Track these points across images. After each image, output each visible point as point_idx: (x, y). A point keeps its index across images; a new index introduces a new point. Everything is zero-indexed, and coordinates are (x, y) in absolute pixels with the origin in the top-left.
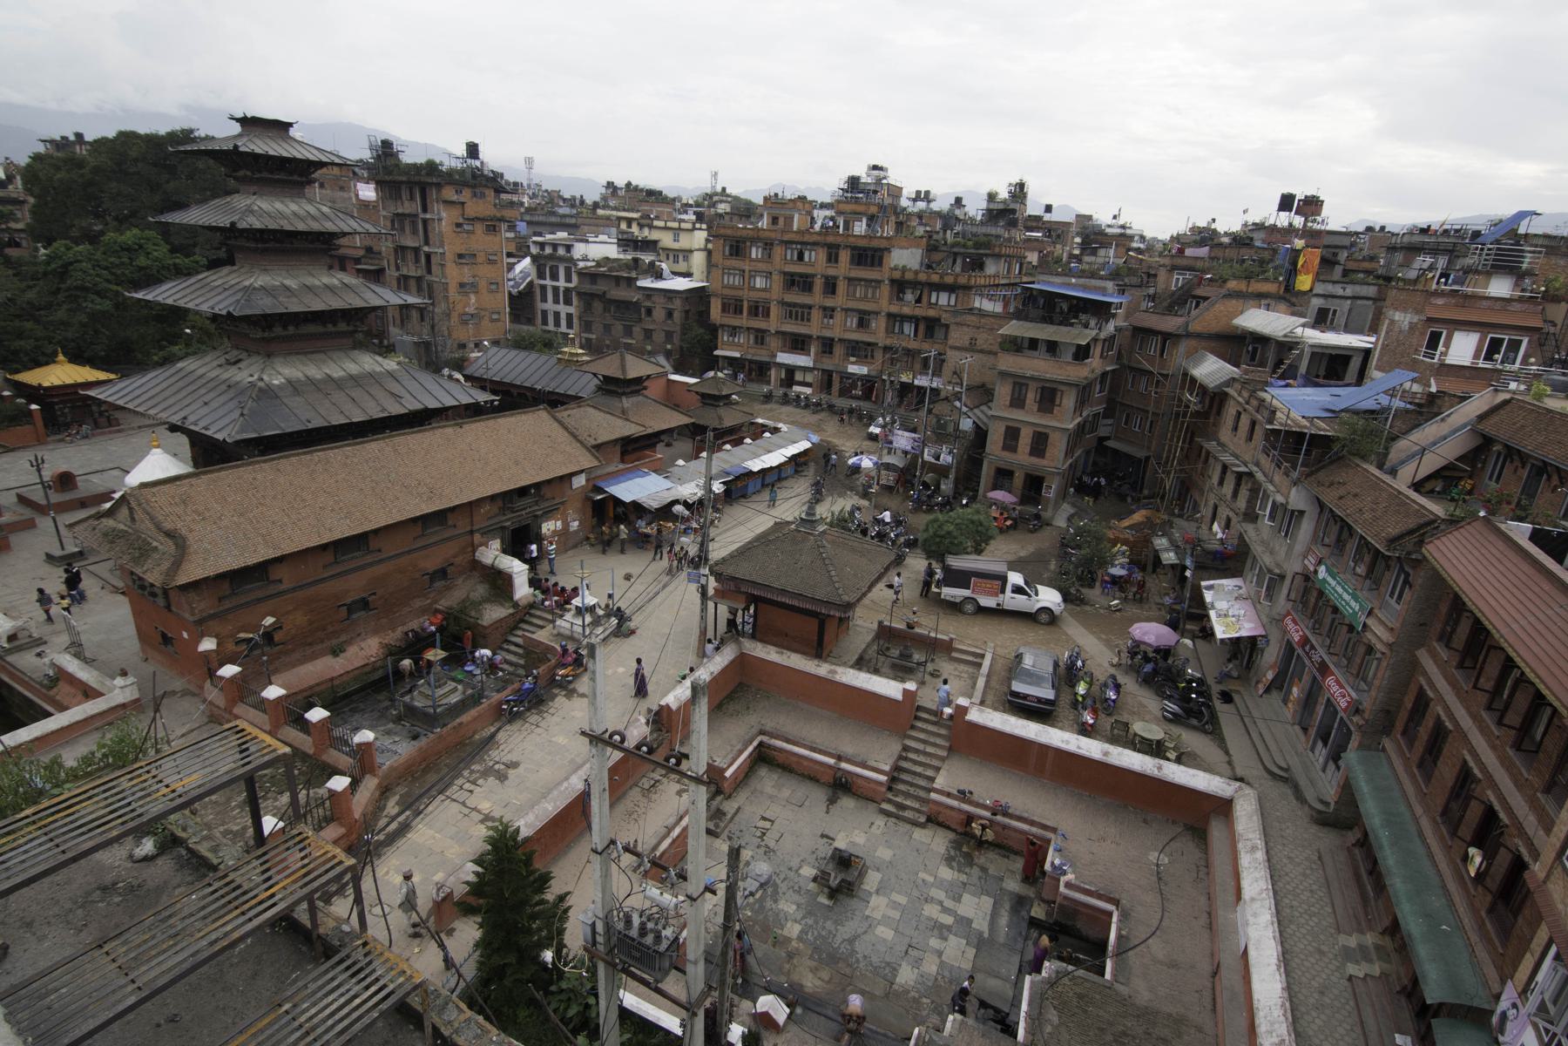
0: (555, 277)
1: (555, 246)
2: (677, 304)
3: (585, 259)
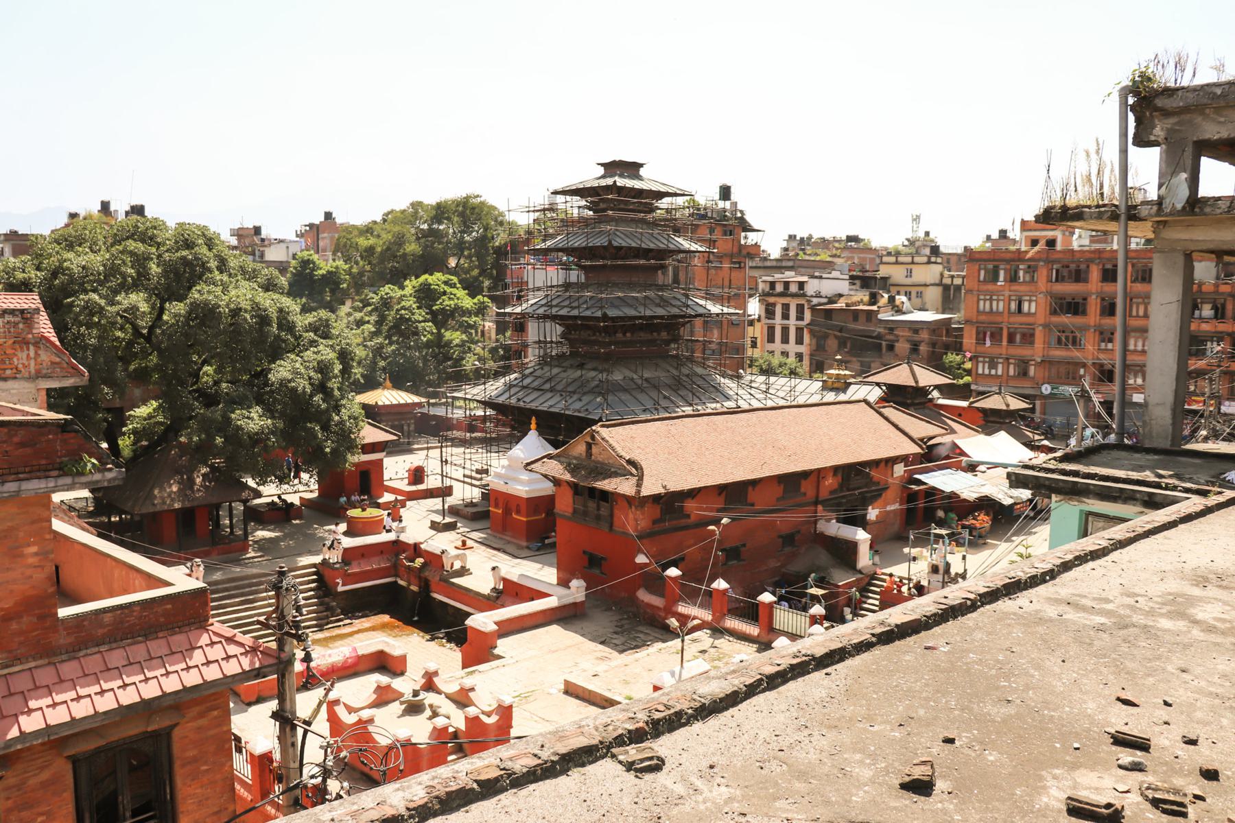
0: (786, 316)
1: (787, 284)
2: (924, 335)
3: (818, 295)
